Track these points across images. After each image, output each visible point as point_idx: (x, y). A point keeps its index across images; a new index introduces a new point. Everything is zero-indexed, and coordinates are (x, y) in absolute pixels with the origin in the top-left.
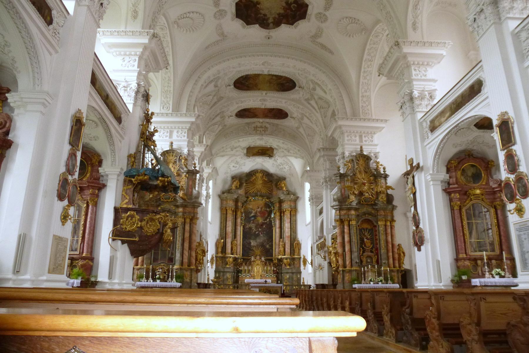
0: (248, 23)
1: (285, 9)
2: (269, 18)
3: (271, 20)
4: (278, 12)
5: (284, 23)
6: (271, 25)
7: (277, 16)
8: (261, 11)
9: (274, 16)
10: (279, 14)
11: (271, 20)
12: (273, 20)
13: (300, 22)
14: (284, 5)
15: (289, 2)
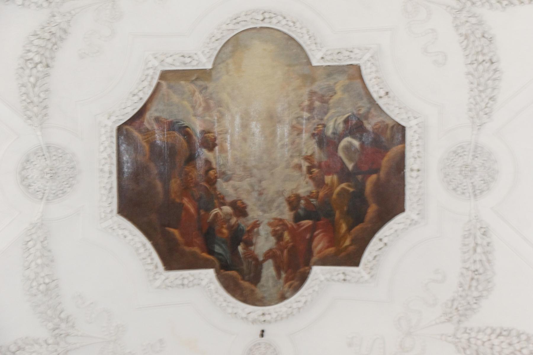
0: (173, 257)
1: (315, 170)
2: (256, 225)
3: (264, 243)
4: (289, 188)
5: (325, 261)
6: (269, 270)
7: (287, 216)
8: (224, 187)
9: (274, 214)
10: (293, 202)
11: (264, 243)
12: (272, 241)
13: (386, 231)
14: (310, 147)
15: (329, 132)
